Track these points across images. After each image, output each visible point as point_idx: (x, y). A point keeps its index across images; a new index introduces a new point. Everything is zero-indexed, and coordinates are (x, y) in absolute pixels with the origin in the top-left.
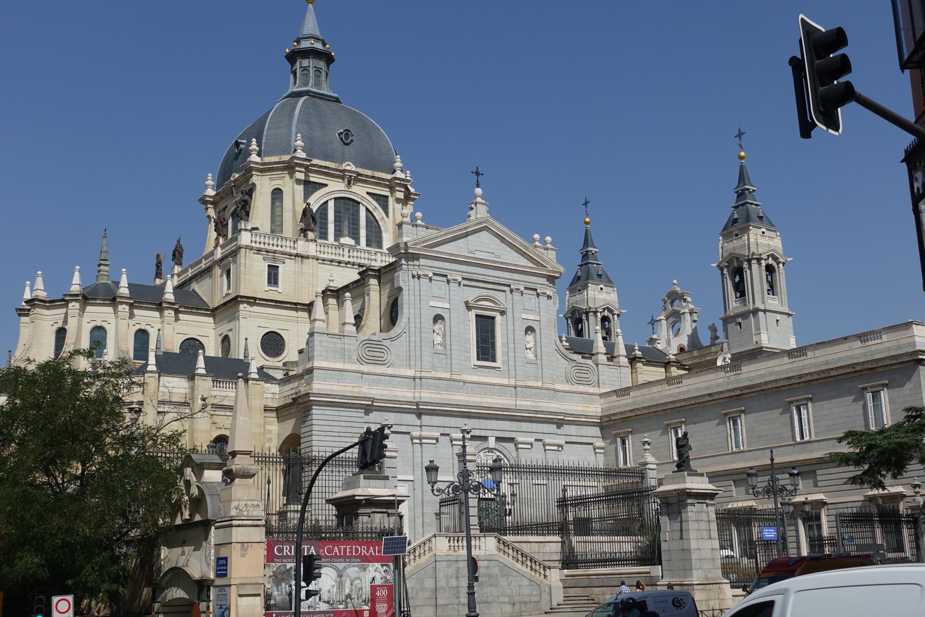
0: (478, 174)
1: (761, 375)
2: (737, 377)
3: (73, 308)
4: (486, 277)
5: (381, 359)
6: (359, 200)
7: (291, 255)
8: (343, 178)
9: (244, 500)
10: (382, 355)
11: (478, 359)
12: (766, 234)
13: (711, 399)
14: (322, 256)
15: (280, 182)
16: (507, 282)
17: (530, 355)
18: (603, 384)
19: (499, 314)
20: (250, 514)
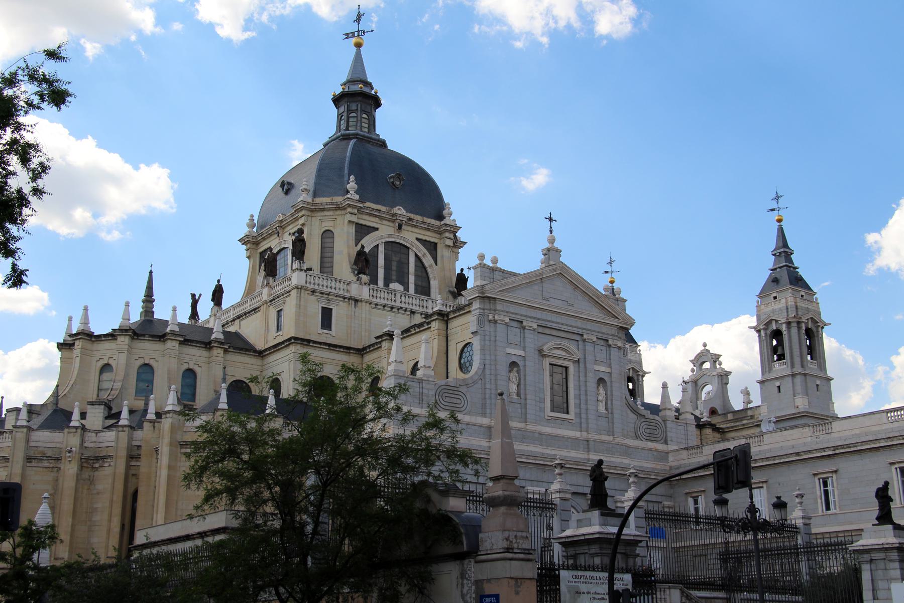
0: (551, 220)
1: (856, 434)
2: (827, 437)
3: (122, 343)
4: (560, 326)
5: (458, 406)
6: (408, 245)
7: (344, 298)
8: (393, 221)
9: (514, 531)
10: (459, 401)
11: (552, 411)
12: (804, 297)
13: (798, 458)
14: (375, 300)
15: (331, 224)
16: (580, 331)
17: (602, 408)
18: (672, 441)
19: (571, 364)
20: (520, 547)
